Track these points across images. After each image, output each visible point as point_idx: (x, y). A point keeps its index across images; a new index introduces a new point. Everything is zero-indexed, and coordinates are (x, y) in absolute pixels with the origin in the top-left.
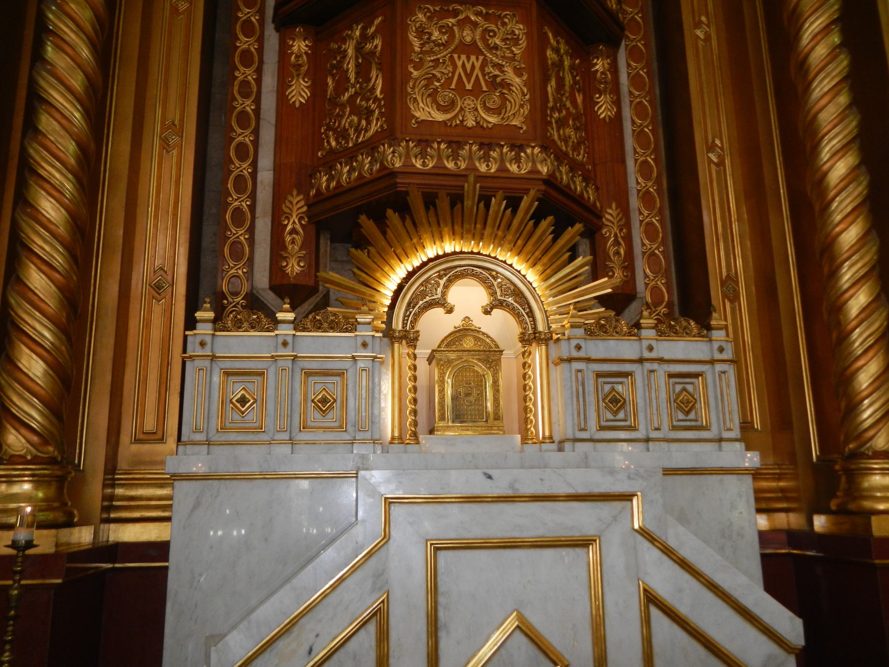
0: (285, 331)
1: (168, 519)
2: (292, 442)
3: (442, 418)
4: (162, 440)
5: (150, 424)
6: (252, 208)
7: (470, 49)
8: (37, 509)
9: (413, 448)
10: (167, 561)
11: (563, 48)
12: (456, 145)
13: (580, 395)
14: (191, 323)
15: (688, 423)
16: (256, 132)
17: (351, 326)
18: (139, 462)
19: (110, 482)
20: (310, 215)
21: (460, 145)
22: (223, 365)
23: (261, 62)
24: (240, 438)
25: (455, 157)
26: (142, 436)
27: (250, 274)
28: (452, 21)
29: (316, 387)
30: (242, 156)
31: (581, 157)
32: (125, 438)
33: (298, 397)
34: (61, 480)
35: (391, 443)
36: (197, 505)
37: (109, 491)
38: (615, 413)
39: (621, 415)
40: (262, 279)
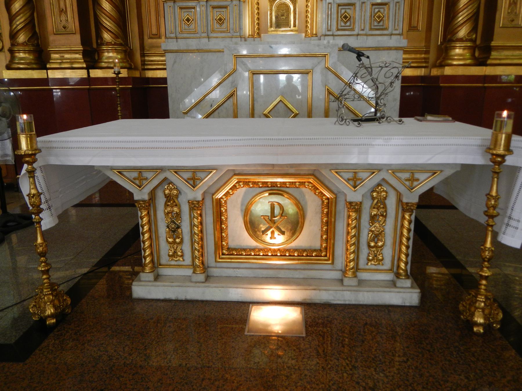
1: (165, 69)
2: (209, 37)
3: (271, 27)
4: (160, 37)
5: (154, 31)
8: (119, 62)
9: (257, 40)
10: (167, 84)
15: (379, 27)
18: (153, 46)
19: (143, 55)
22: (178, 5)
24: (188, 36)
26: (152, 36)
29: (217, 14)
32: (146, 37)
33: (210, 18)
34: (125, 52)
35: (248, 37)
36: (175, 62)
37: (143, 59)
38: (346, 23)
39: (348, 24)
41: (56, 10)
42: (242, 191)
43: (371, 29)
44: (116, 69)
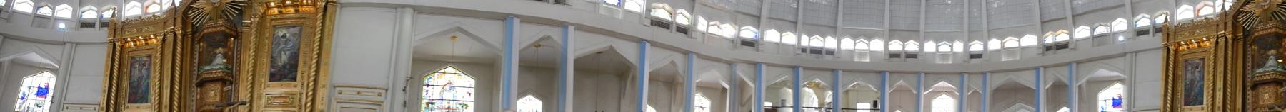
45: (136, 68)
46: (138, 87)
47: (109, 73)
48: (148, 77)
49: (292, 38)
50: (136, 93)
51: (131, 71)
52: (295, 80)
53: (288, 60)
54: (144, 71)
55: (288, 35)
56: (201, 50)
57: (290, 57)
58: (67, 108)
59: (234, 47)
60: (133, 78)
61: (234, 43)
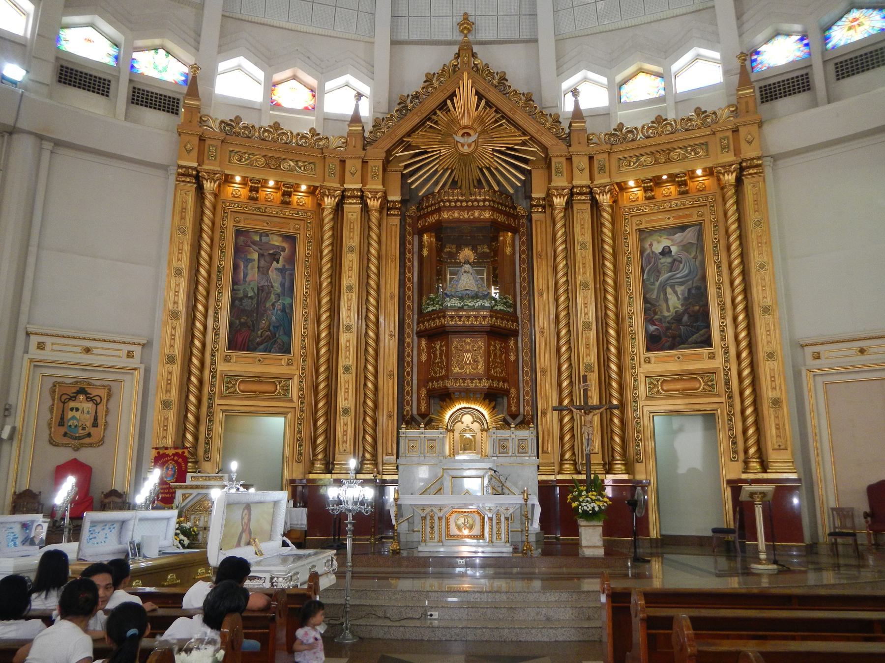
0: (422, 430)
6: (412, 390)
7: (468, 351)
11: (498, 342)
12: (464, 380)
13: (494, 446)
14: (399, 428)
16: (412, 367)
17: (438, 429)
20: (427, 393)
21: (465, 379)
23: (413, 347)
25: (464, 383)
27: (411, 409)
28: (463, 344)
29: (430, 444)
30: (408, 375)
31: (503, 375)
40: (415, 412)
41: (341, 442)
42: (455, 515)
43: (518, 453)
44: (375, 474)
45: (248, 261)
46: (259, 310)
47: (184, 265)
48: (289, 290)
49: (684, 256)
50: (253, 328)
51: (236, 268)
52: (710, 345)
53: (682, 305)
54: (273, 275)
55: (674, 249)
56: (425, 252)
57: (686, 299)
58: (41, 346)
59: (514, 254)
60: (241, 288)
61: (513, 240)
